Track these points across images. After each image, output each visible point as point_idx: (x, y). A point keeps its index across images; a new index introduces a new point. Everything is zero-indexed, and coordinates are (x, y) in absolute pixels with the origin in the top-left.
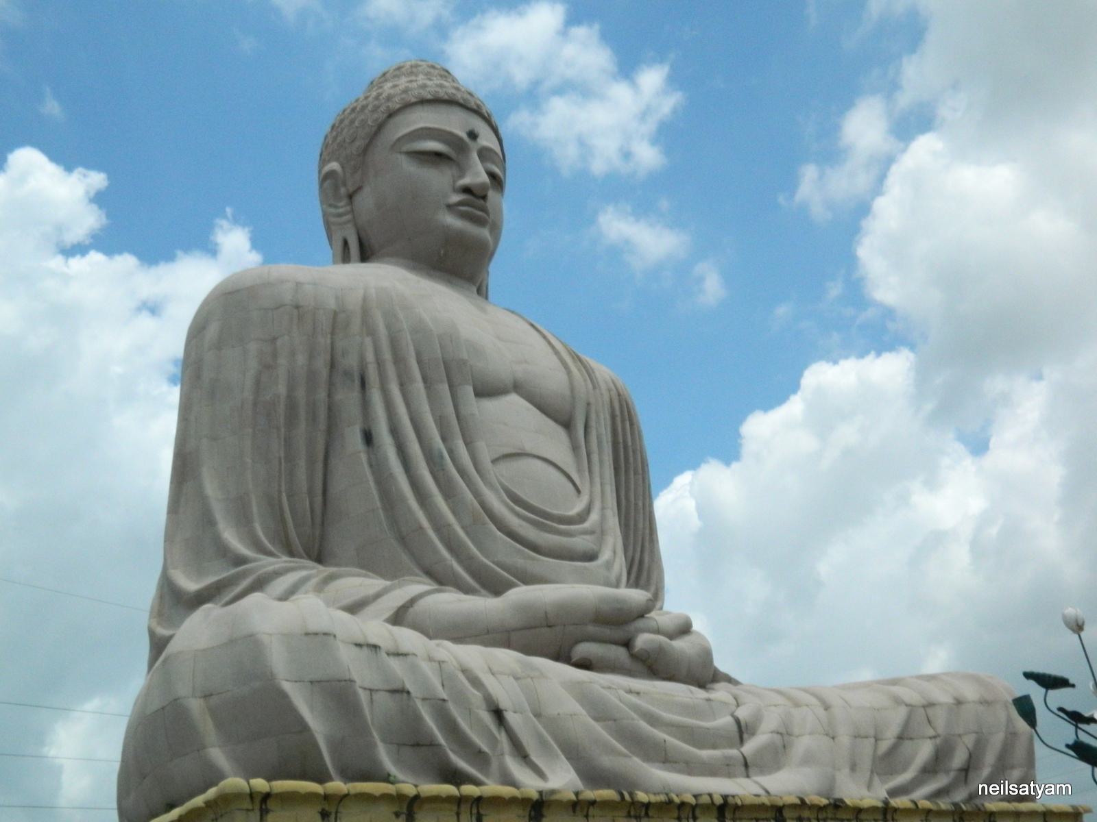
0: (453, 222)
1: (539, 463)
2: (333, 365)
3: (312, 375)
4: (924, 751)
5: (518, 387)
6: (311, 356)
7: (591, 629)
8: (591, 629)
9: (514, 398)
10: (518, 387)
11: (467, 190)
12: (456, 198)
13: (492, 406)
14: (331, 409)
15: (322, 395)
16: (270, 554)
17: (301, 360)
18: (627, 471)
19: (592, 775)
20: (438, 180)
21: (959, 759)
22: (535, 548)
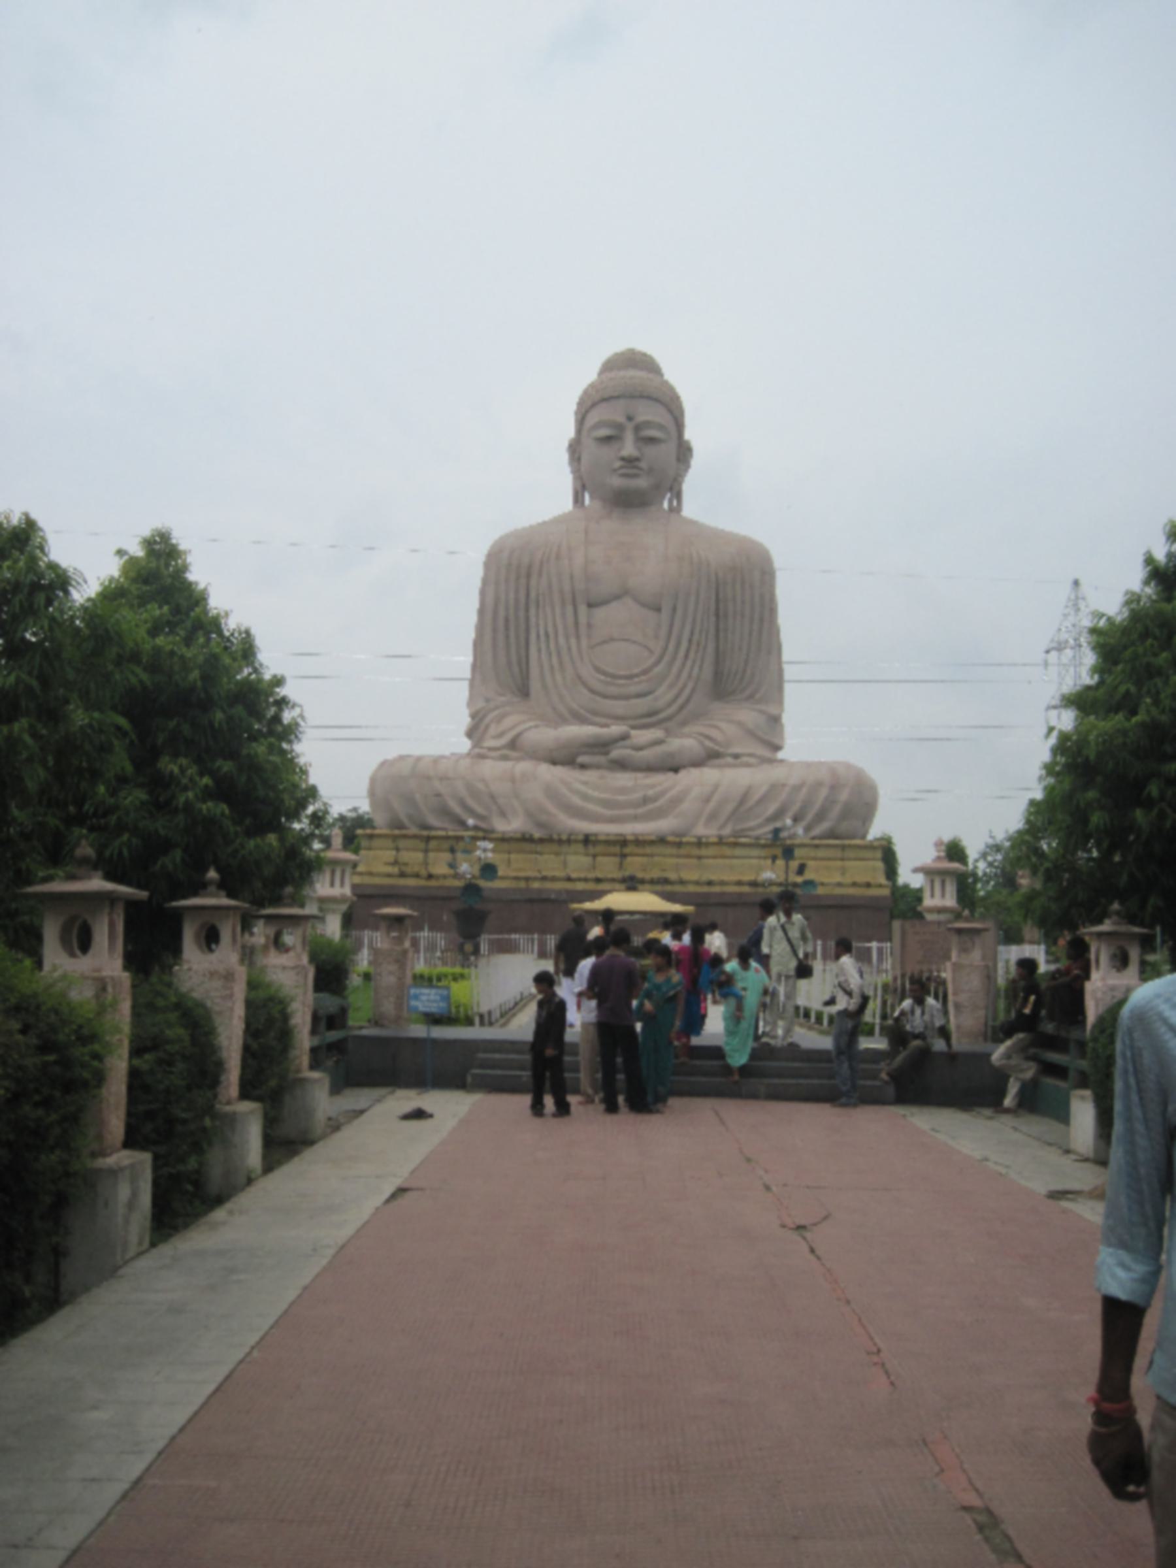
0: (616, 482)
2: (528, 595)
3: (517, 600)
4: (772, 808)
6: (517, 591)
9: (628, 601)
11: (623, 459)
12: (618, 464)
13: (600, 613)
14: (527, 619)
15: (522, 614)
17: (512, 596)
19: (540, 825)
20: (607, 453)
21: (790, 813)
22: (605, 697)
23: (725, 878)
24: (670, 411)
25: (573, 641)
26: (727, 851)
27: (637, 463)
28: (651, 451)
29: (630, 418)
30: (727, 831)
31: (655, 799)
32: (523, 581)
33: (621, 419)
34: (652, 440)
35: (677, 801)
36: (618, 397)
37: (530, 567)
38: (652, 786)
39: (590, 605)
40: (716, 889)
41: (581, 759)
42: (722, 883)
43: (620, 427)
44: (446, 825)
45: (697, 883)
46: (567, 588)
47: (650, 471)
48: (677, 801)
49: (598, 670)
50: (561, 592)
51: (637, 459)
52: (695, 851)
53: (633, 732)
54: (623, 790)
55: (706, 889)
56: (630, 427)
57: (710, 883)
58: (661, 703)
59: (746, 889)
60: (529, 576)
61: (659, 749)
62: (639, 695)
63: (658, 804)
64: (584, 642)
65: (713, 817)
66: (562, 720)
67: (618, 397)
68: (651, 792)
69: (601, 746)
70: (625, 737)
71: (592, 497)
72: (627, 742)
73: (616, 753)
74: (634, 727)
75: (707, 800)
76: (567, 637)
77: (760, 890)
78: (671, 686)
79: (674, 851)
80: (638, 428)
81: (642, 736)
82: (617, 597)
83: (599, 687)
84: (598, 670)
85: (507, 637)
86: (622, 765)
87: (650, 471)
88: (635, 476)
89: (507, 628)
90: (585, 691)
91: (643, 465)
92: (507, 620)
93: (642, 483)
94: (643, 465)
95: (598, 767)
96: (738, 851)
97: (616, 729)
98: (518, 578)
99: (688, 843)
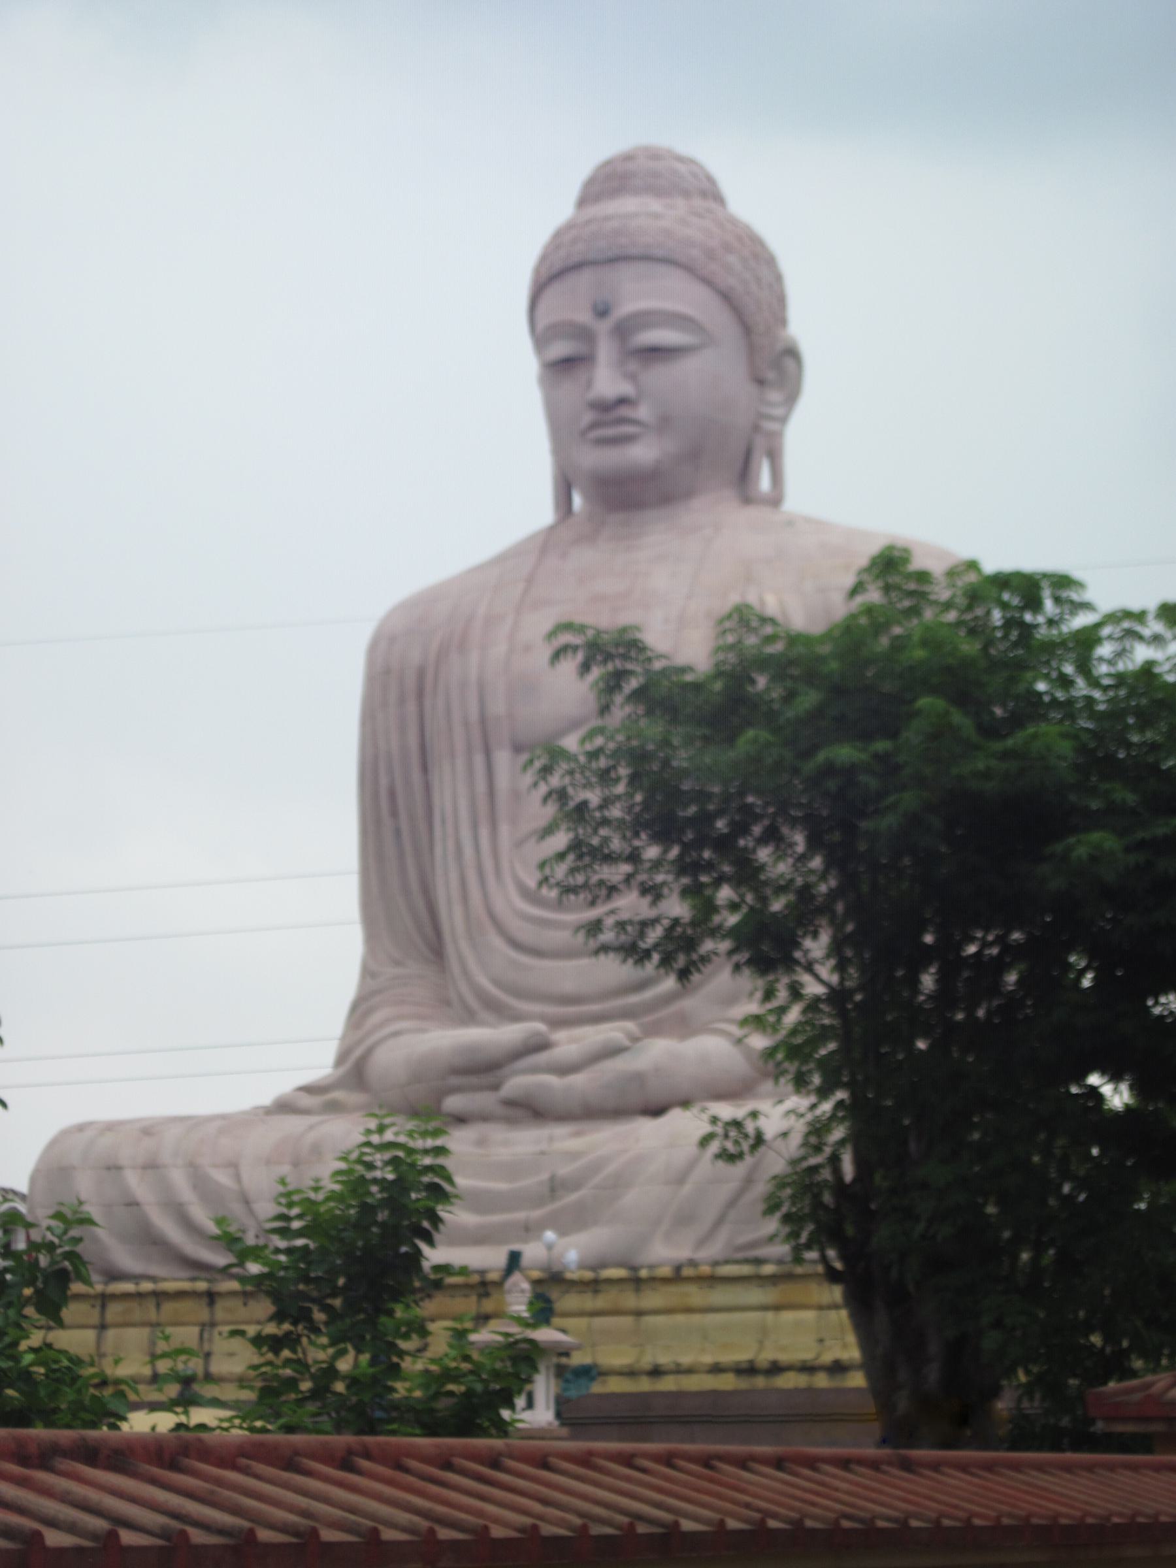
7: (454, 1081)
8: (454, 1081)
12: (588, 417)
16: (397, 963)
23: (686, 1360)
24: (707, 281)
25: (484, 833)
26: (696, 1295)
27: (624, 411)
28: (659, 376)
29: (602, 312)
30: (714, 1250)
31: (574, 1183)
32: (411, 708)
33: (584, 316)
34: (656, 353)
35: (618, 1184)
36: (578, 266)
37: (421, 673)
38: (574, 1156)
40: (668, 1384)
41: (453, 1103)
42: (680, 1370)
43: (585, 335)
44: (155, 1270)
45: (631, 1373)
46: (474, 716)
47: (664, 423)
48: (618, 1184)
50: (466, 724)
51: (622, 401)
52: (630, 1300)
53: (560, 1035)
54: (512, 1170)
55: (645, 1385)
56: (603, 328)
57: (656, 1372)
59: (727, 1382)
60: (420, 694)
61: (620, 1065)
63: (583, 1192)
64: (504, 829)
65: (684, 1219)
66: (469, 1018)
67: (578, 266)
68: (565, 1170)
69: (483, 1069)
70: (541, 1045)
71: (586, 497)
72: (542, 1057)
73: (517, 1083)
74: (558, 1023)
75: (681, 1179)
76: (475, 826)
77: (760, 1382)
79: (589, 1302)
81: (571, 1043)
83: (526, 933)
85: (398, 832)
86: (531, 1111)
89: (394, 814)
90: (497, 942)
91: (643, 412)
92: (392, 795)
93: (643, 453)
94: (643, 412)
95: (485, 1118)
96: (720, 1296)
97: (508, 1034)
98: (402, 701)
99: (609, 1281)
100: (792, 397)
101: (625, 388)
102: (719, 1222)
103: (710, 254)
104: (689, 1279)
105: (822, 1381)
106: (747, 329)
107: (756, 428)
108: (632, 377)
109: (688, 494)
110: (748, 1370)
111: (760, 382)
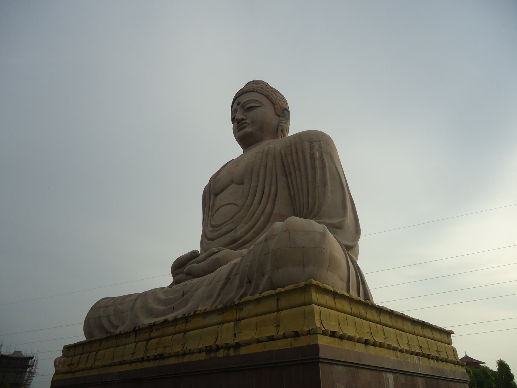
1: (224, 207)
5: (232, 182)
9: (233, 185)
10: (232, 182)
18: (295, 172)
22: (212, 240)
24: (262, 94)
34: (250, 108)
39: (216, 195)
47: (253, 123)
49: (212, 226)
51: (243, 119)
58: (239, 233)
62: (226, 233)
78: (247, 223)
80: (243, 107)
82: (227, 186)
84: (212, 226)
87: (253, 123)
88: (245, 127)
93: (248, 129)
94: (247, 121)
100: (288, 118)
101: (243, 117)
102: (218, 296)
103: (263, 89)
104: (198, 315)
105: (232, 353)
106: (273, 104)
107: (278, 125)
108: (246, 116)
109: (262, 140)
110: (209, 350)
111: (279, 116)
